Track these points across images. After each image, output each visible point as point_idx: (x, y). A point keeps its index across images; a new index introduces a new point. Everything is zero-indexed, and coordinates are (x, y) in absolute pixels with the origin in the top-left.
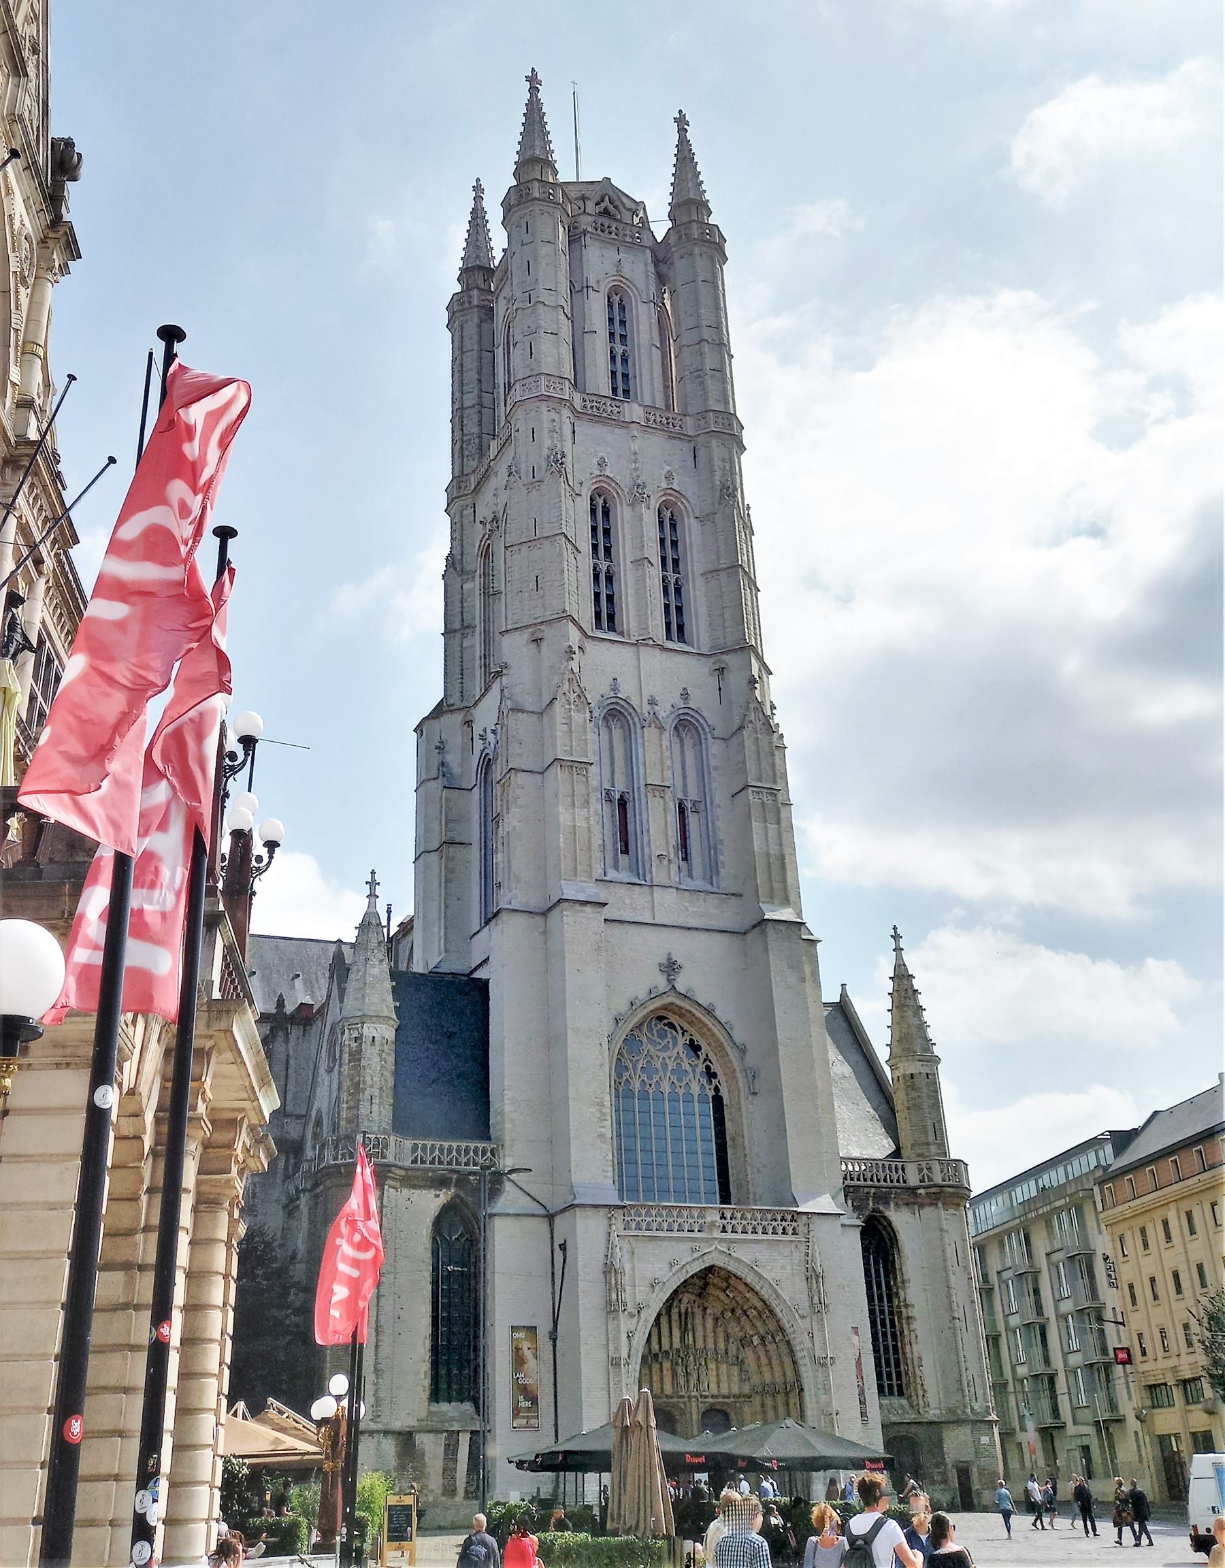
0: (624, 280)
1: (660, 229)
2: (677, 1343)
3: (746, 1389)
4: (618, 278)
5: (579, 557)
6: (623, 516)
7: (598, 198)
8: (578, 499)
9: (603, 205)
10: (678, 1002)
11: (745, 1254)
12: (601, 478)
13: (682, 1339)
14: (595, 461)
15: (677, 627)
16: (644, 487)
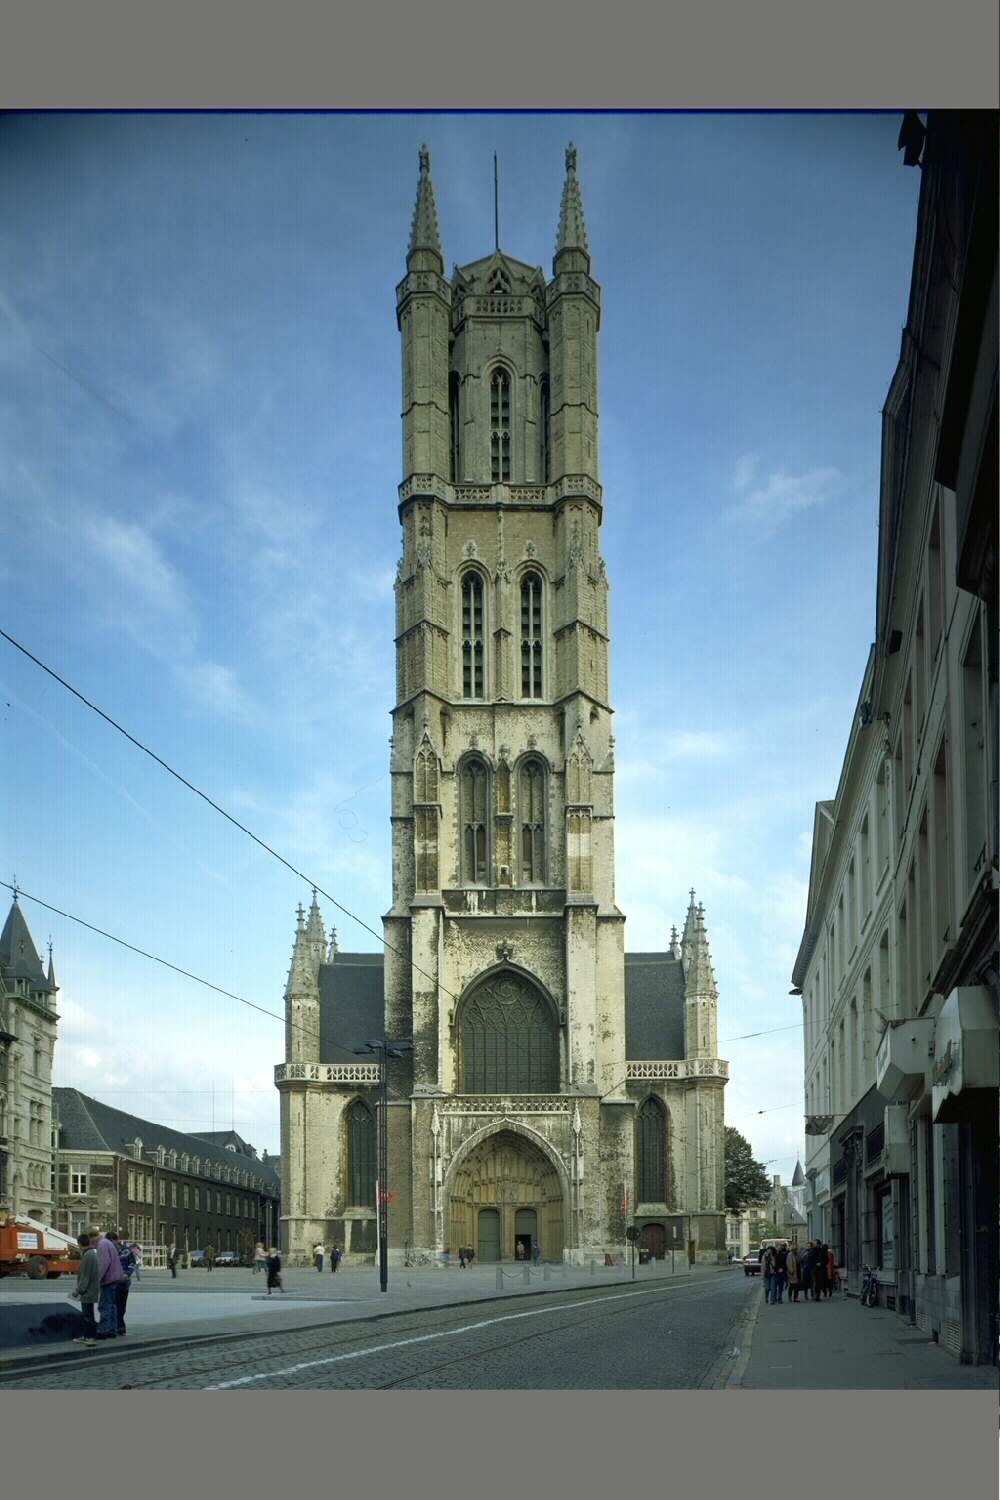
0: (504, 360)
1: (548, 277)
2: (499, 1174)
3: (544, 1200)
4: (499, 358)
5: (449, 638)
6: (488, 593)
7: (489, 274)
8: (450, 586)
9: (495, 281)
10: (510, 968)
11: (525, 1124)
12: (469, 563)
13: (503, 1170)
14: (464, 548)
15: (532, 683)
16: (504, 564)
